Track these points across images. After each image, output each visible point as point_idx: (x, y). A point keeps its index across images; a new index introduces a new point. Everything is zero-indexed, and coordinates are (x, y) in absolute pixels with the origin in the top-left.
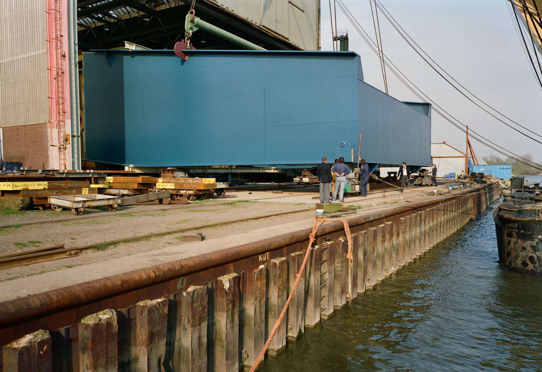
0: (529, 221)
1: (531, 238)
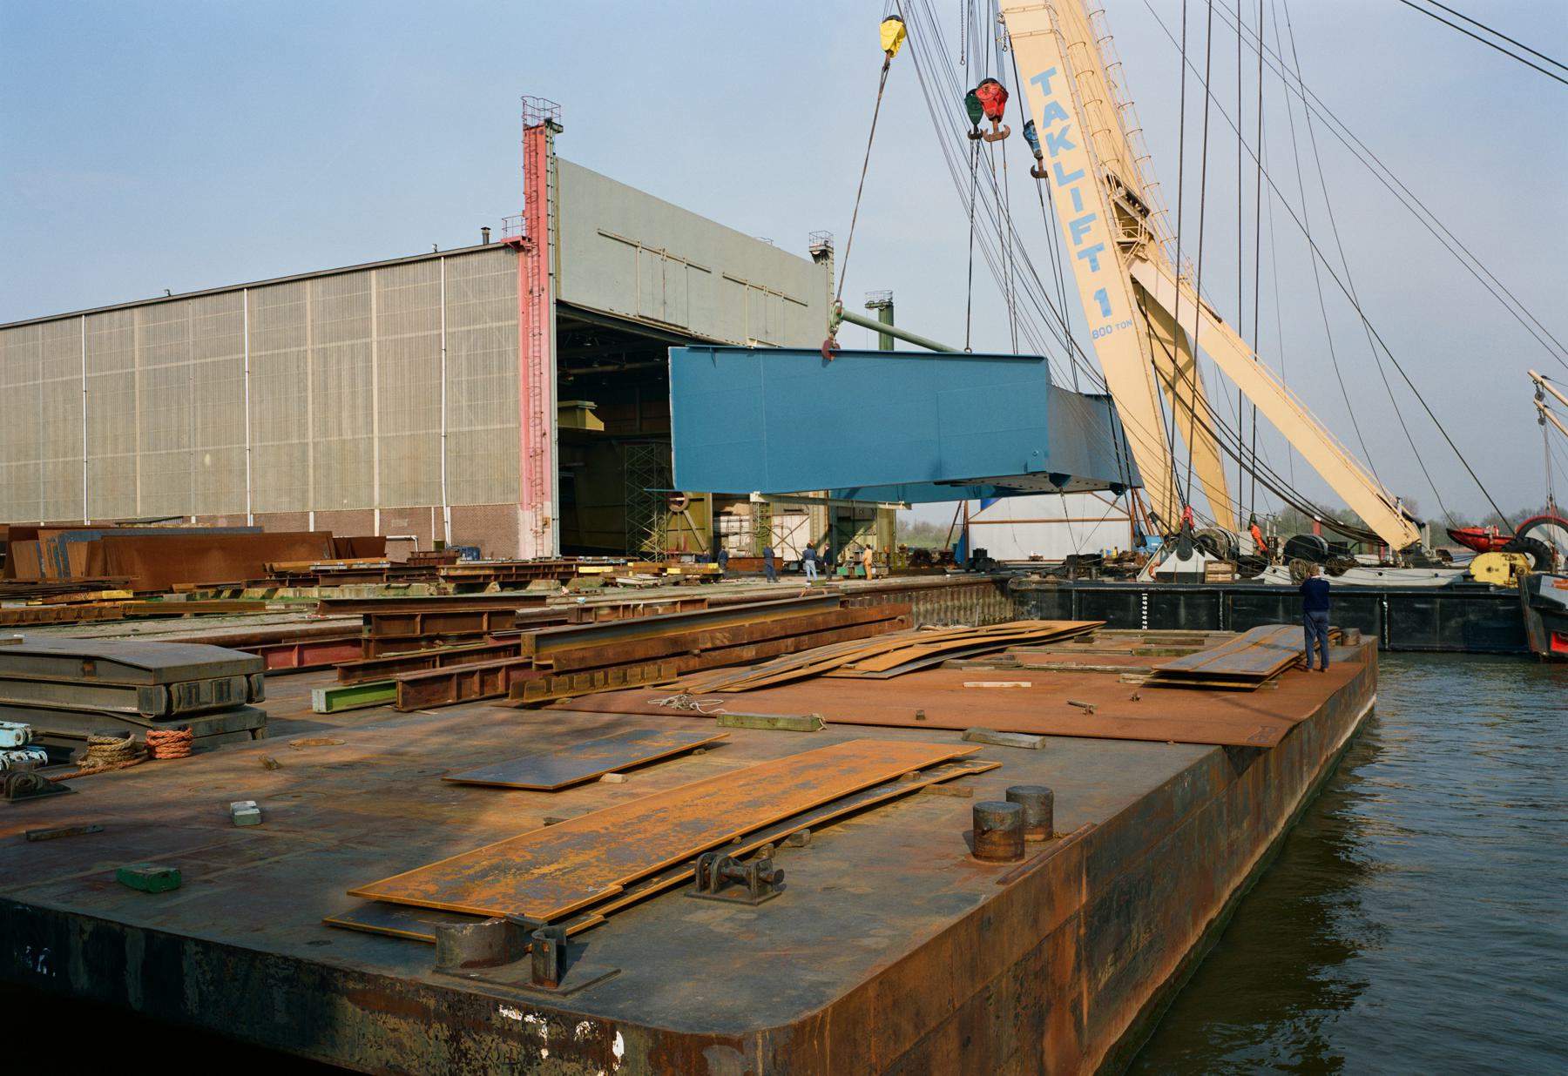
0: (1025, 590)
1: (1027, 605)
